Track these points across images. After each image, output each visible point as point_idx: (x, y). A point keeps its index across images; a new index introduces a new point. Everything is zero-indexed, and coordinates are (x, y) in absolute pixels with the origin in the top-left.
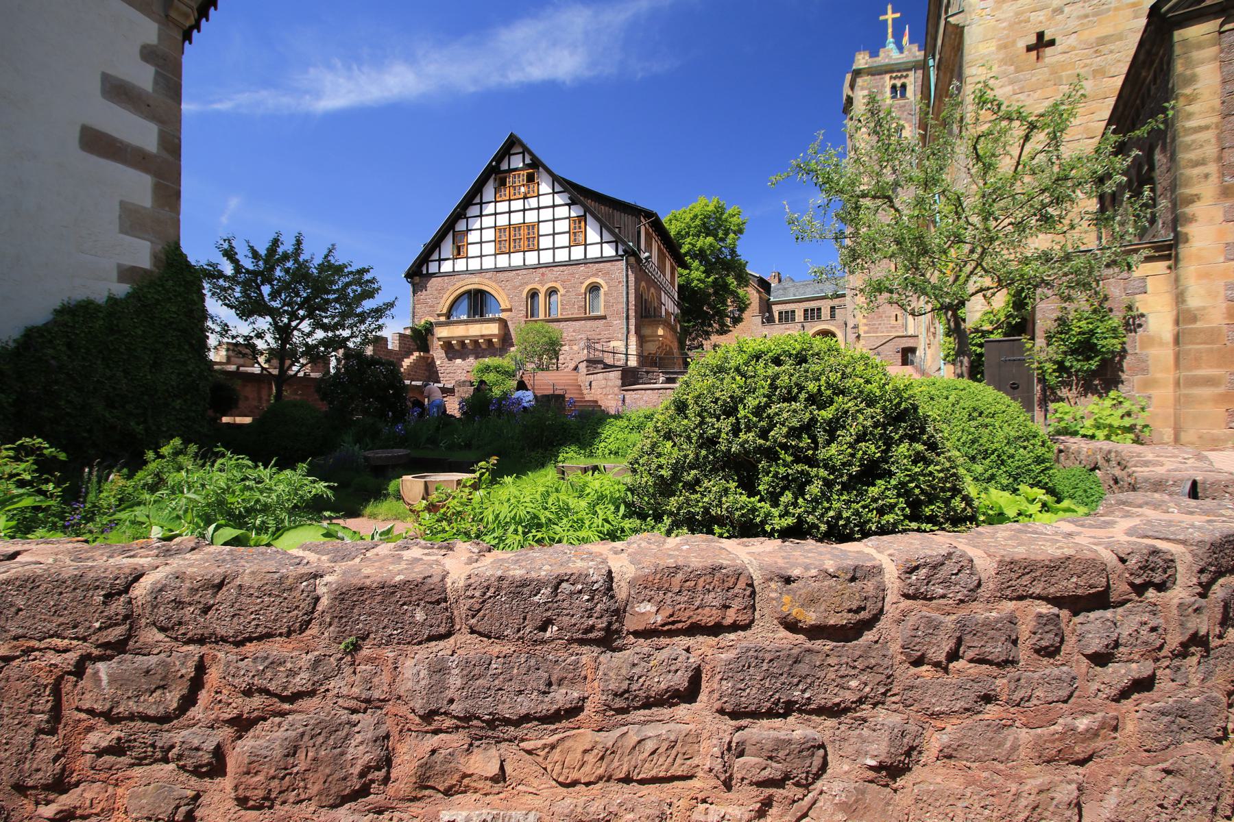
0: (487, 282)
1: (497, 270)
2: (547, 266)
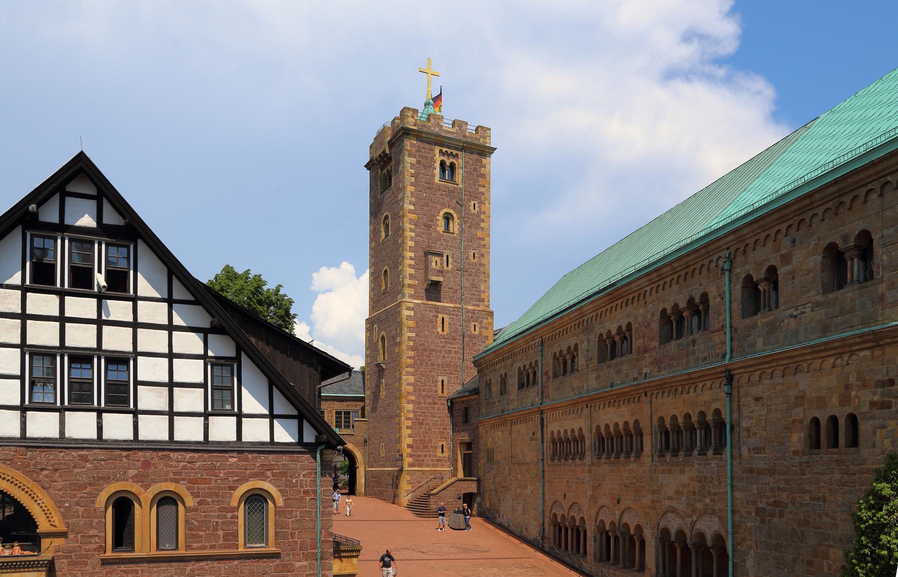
2: (154, 446)
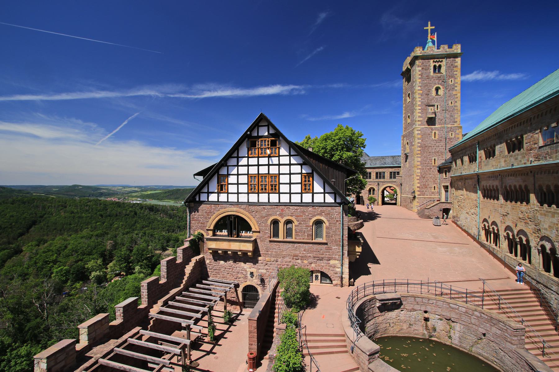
0: (242, 211)
1: (249, 203)
2: (285, 204)
